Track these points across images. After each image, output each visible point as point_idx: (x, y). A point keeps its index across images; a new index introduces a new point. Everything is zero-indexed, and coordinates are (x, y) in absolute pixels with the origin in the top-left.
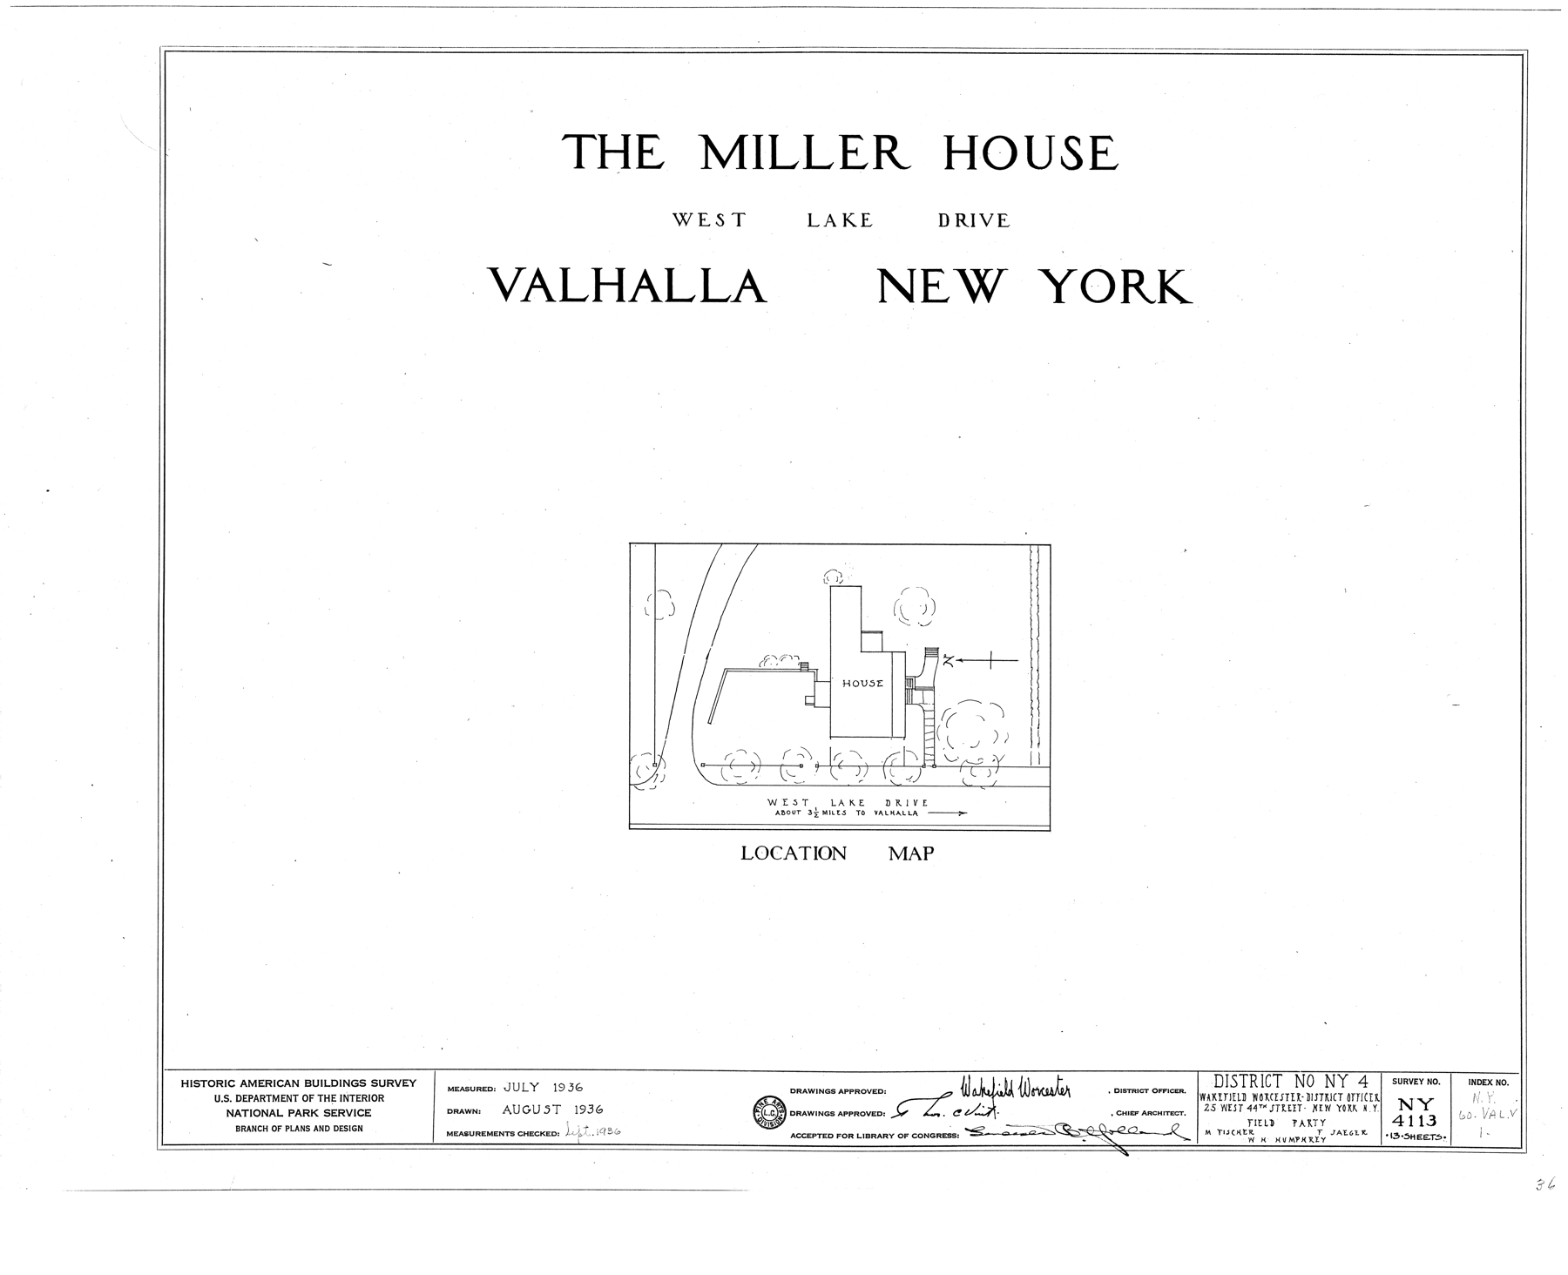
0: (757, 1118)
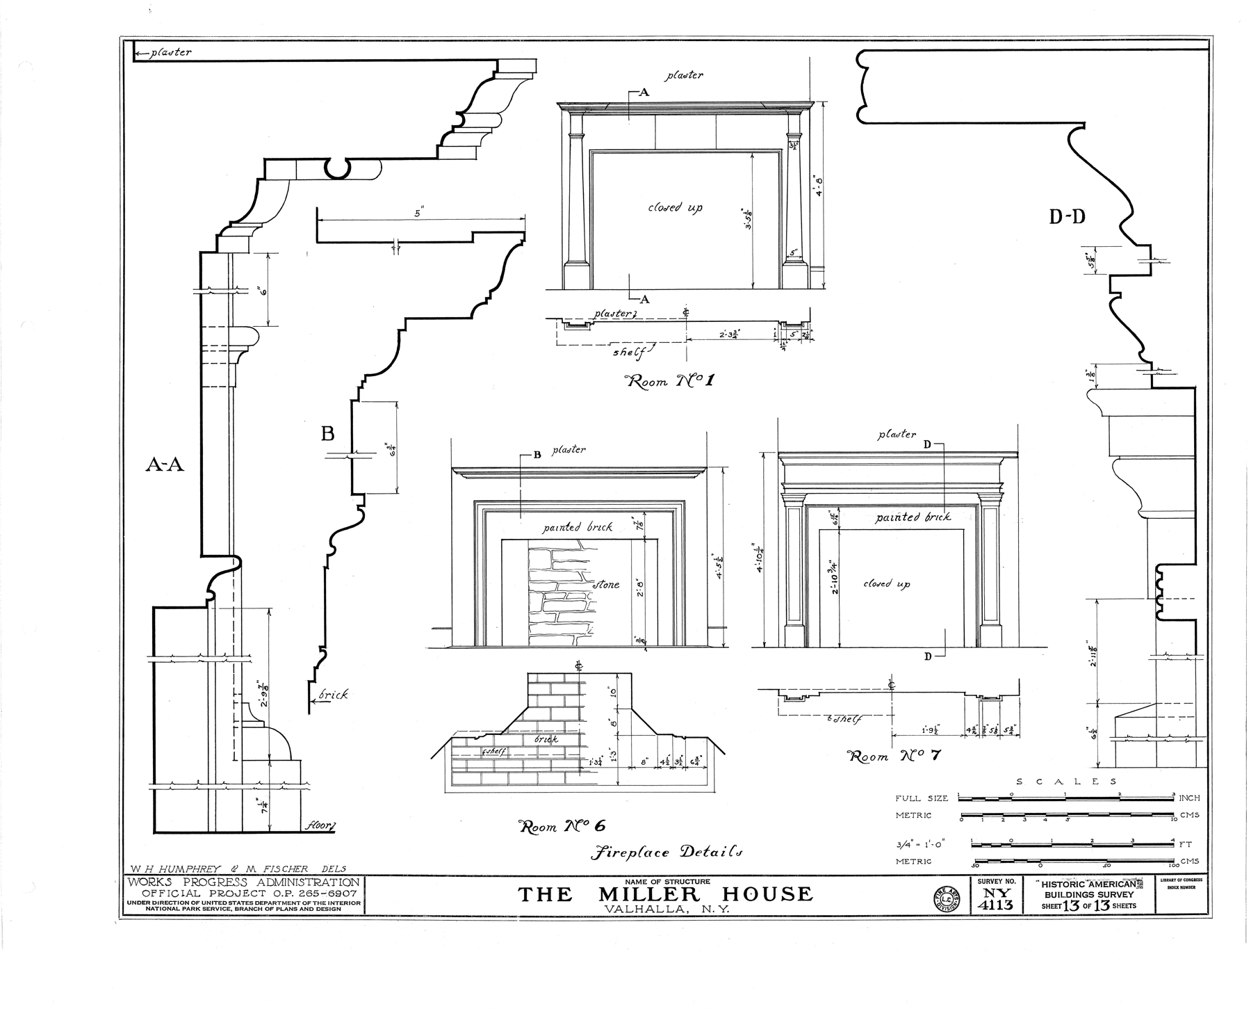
0: (937, 903)
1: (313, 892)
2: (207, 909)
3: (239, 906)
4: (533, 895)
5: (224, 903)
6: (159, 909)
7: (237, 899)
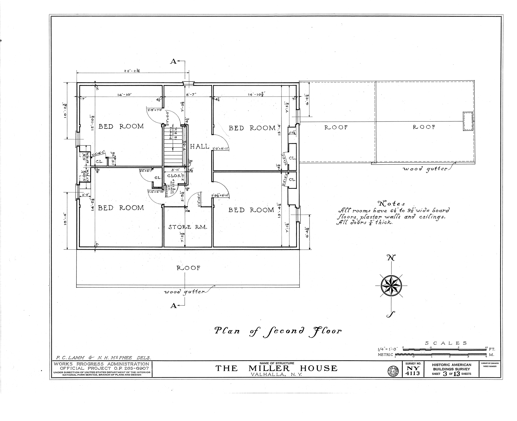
0: (389, 373)
1: (130, 368)
2: (88, 375)
3: (100, 373)
4: (222, 369)
5: (94, 372)
6: (68, 375)
7: (99, 371)
